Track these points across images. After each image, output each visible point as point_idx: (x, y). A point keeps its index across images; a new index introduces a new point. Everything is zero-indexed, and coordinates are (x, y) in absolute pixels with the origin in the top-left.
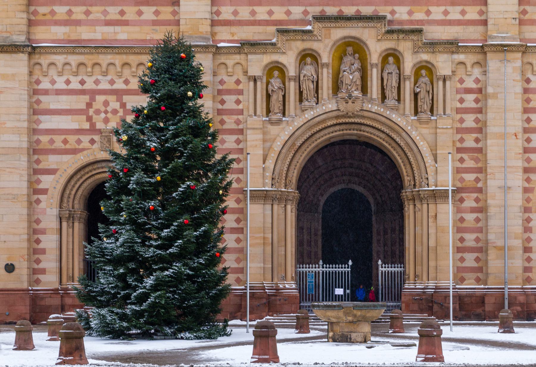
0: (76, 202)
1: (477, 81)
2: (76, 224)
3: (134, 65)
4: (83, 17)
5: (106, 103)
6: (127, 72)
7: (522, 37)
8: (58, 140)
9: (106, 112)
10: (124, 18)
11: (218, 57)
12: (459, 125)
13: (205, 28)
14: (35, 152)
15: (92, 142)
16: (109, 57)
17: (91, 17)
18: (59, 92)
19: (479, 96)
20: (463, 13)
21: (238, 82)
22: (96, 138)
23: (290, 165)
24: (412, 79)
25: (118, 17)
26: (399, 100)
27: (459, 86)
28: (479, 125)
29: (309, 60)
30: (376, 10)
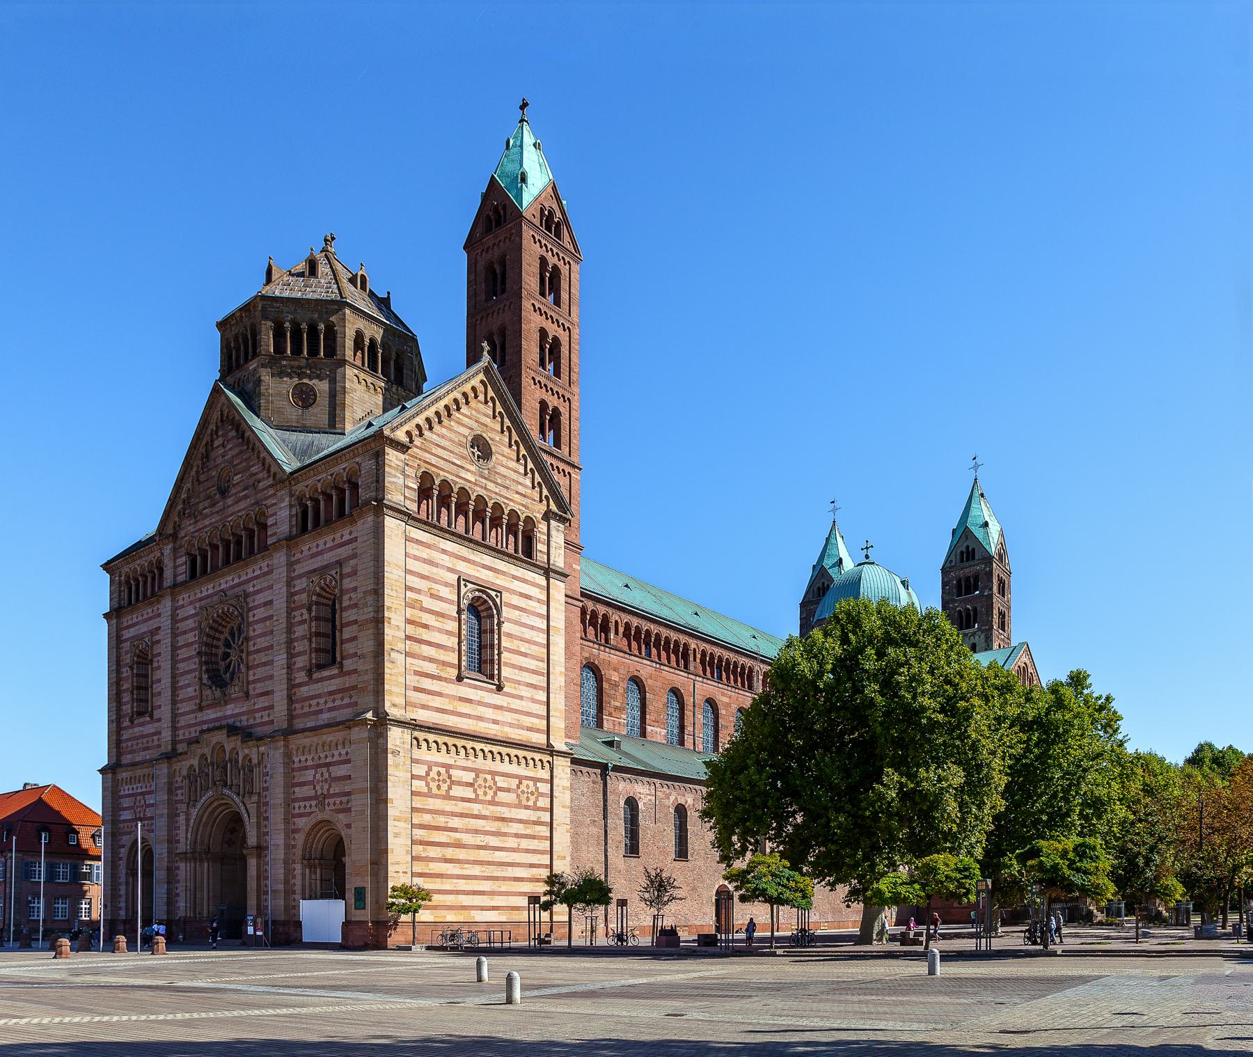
10: (149, 745)
13: (170, 747)
21: (182, 781)
30: (234, 722)
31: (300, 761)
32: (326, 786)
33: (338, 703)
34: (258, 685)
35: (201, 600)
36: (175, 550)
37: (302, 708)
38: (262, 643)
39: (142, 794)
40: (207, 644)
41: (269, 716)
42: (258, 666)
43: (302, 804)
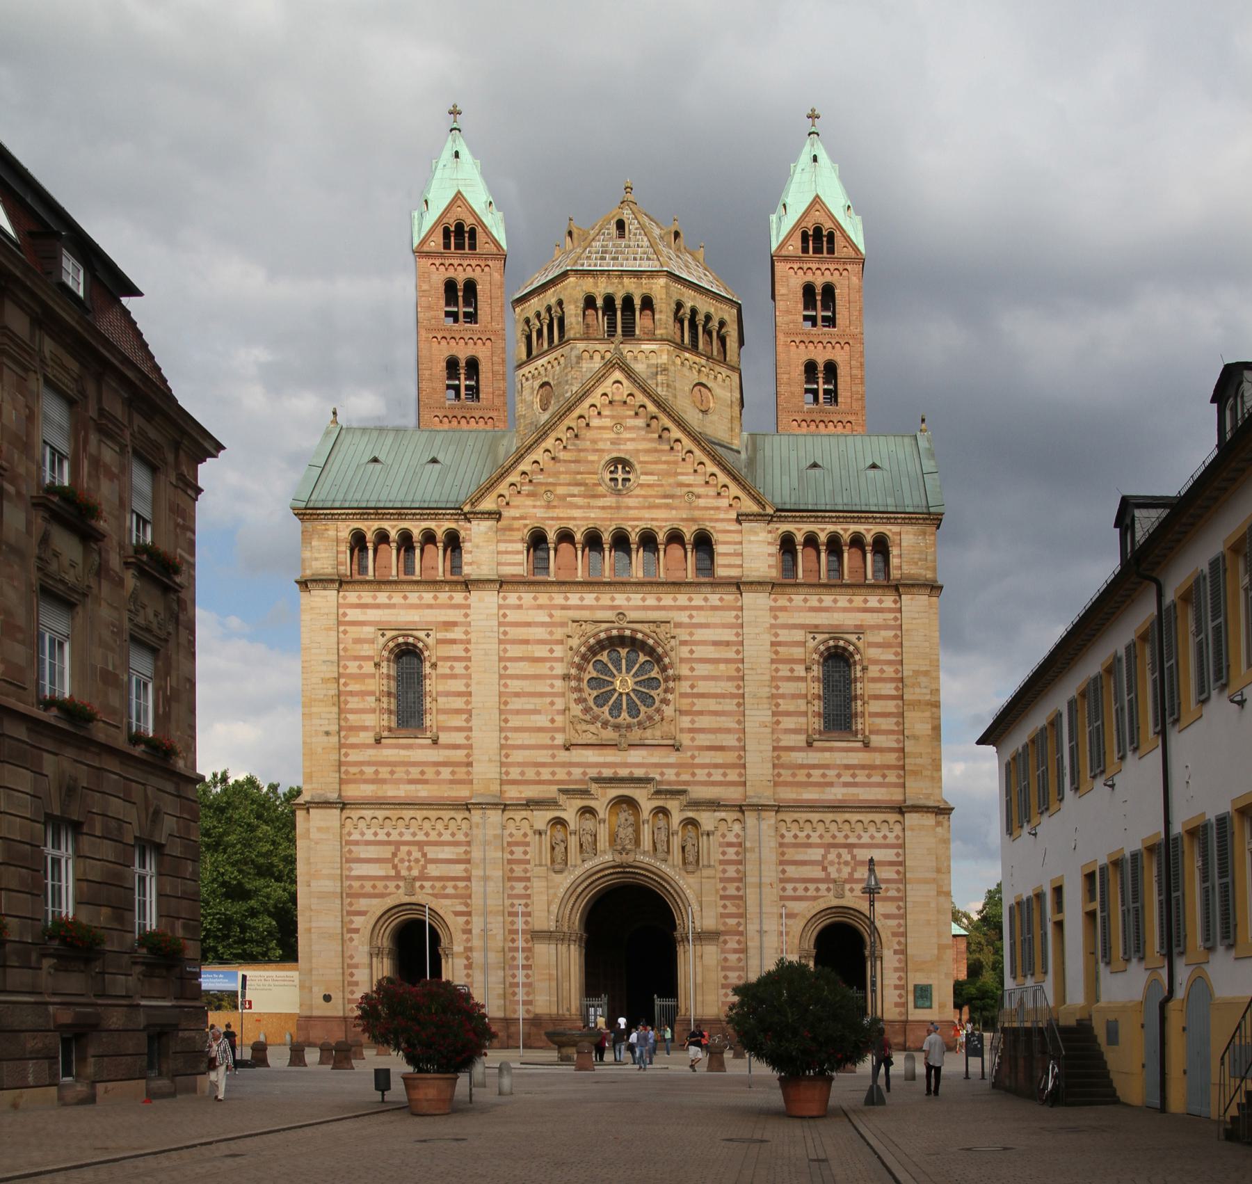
0: (385, 940)
1: (737, 836)
2: (385, 960)
3: (433, 819)
4: (388, 776)
5: (409, 853)
6: (427, 825)
7: (776, 797)
8: (368, 884)
9: (409, 861)
11: (506, 813)
12: (722, 875)
13: (495, 787)
14: (348, 895)
15: (398, 887)
16: (411, 812)
17: (395, 776)
18: (368, 843)
19: (740, 850)
20: (725, 775)
21: (525, 835)
22: (401, 884)
23: (572, 909)
24: (680, 833)
25: (420, 777)
26: (668, 852)
27: (721, 840)
28: (740, 875)
29: (587, 815)
30: (647, 772)
31: (796, 836)
32: (846, 870)
33: (861, 778)
34: (702, 736)
35: (564, 608)
36: (498, 530)
37: (794, 775)
38: (702, 687)
39: (420, 845)
40: (580, 668)
41: (725, 775)
42: (701, 713)
43: (801, 886)
